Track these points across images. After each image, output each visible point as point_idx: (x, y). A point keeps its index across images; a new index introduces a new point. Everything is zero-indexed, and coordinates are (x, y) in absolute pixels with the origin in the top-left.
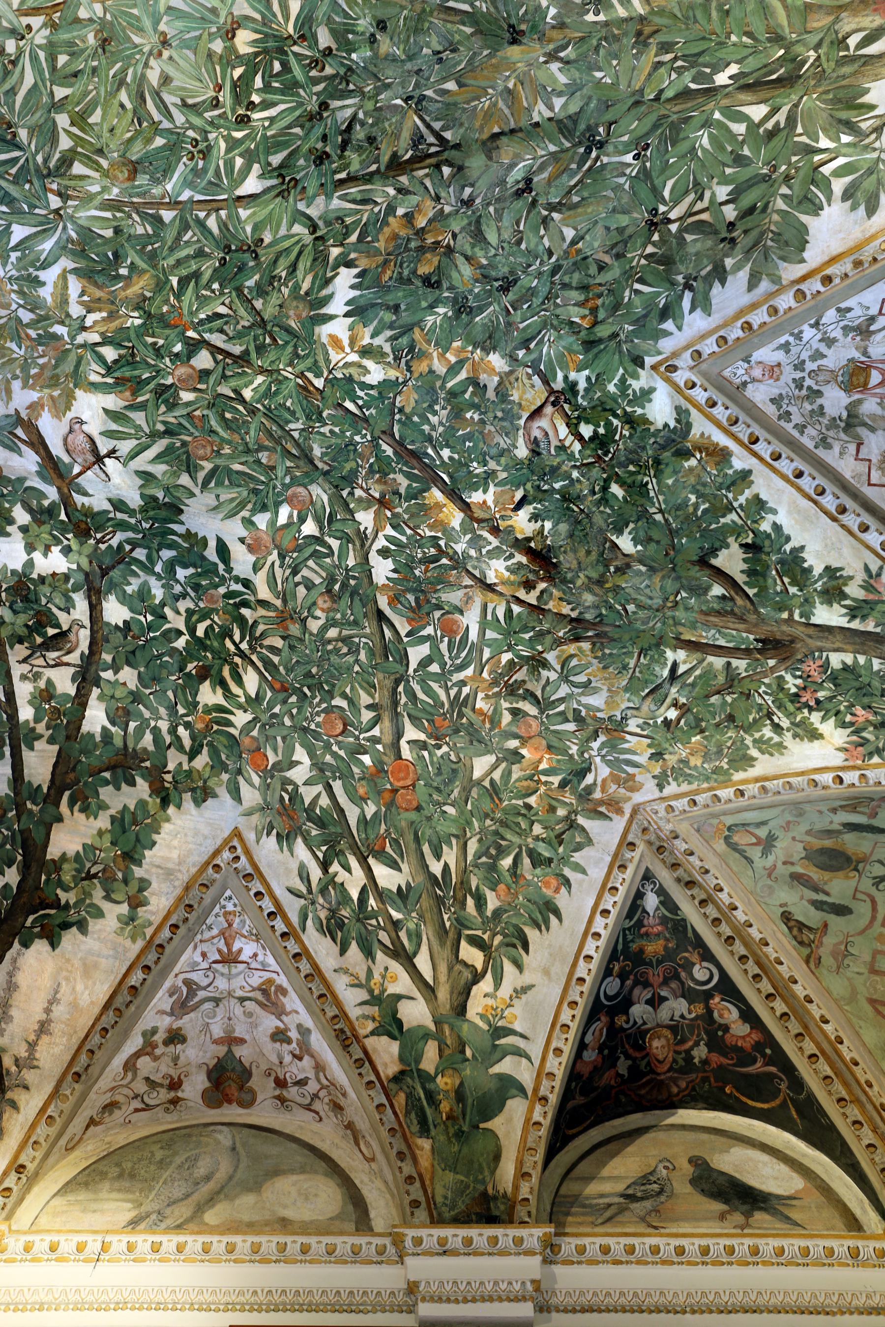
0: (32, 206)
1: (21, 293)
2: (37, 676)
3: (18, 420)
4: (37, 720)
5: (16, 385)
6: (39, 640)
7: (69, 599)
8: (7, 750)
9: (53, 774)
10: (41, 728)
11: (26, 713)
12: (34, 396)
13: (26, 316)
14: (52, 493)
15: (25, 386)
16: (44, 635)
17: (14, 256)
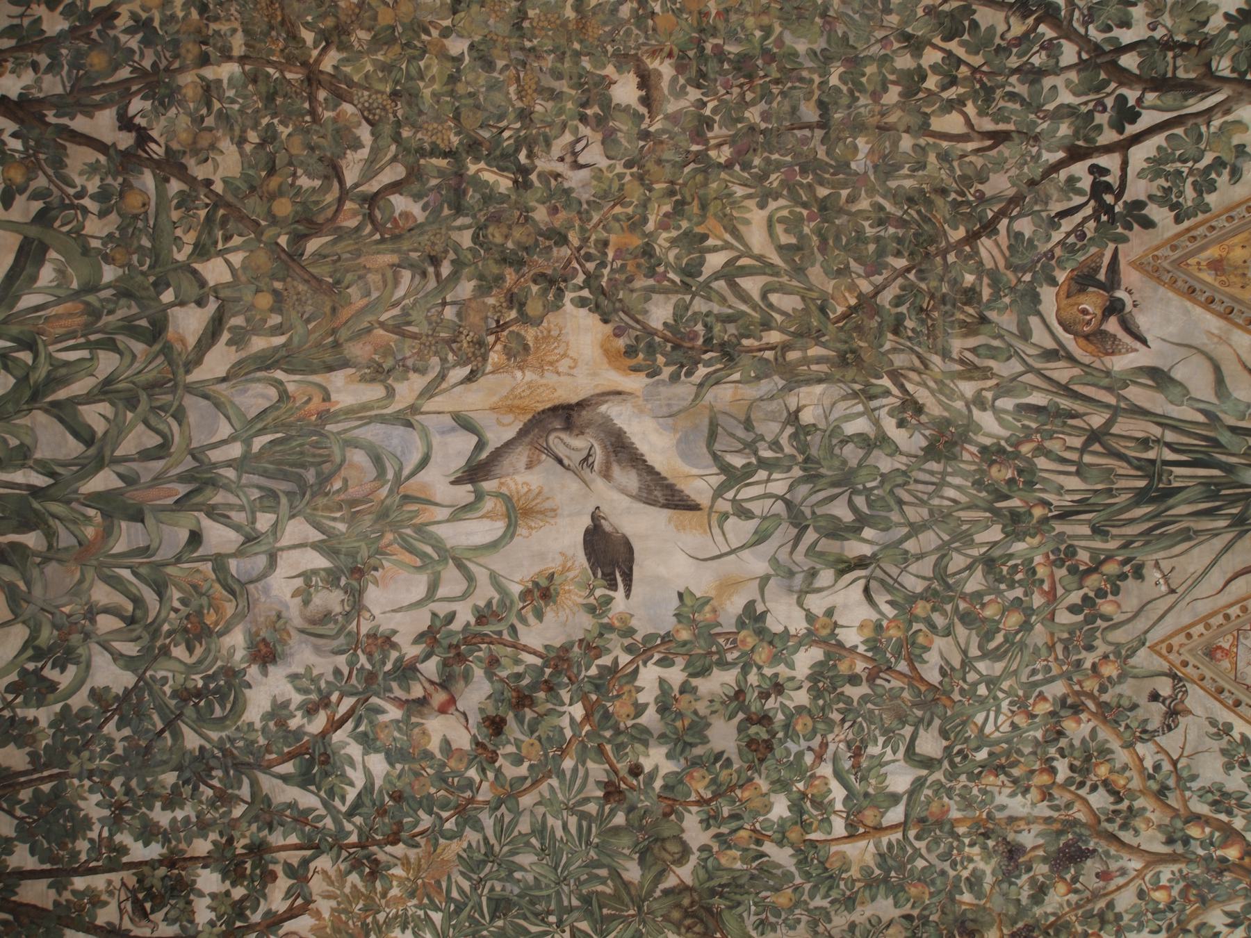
0: (454, 927)
1: (396, 916)
2: (111, 893)
3: (308, 901)
4: (74, 892)
5: (333, 903)
6: (141, 896)
7: (174, 922)
8: (47, 866)
9: (27, 905)
10: (67, 895)
11: (79, 883)
12: (326, 915)
13: (381, 917)
14: (256, 918)
15: (333, 910)
16: (145, 900)
17: (421, 913)
